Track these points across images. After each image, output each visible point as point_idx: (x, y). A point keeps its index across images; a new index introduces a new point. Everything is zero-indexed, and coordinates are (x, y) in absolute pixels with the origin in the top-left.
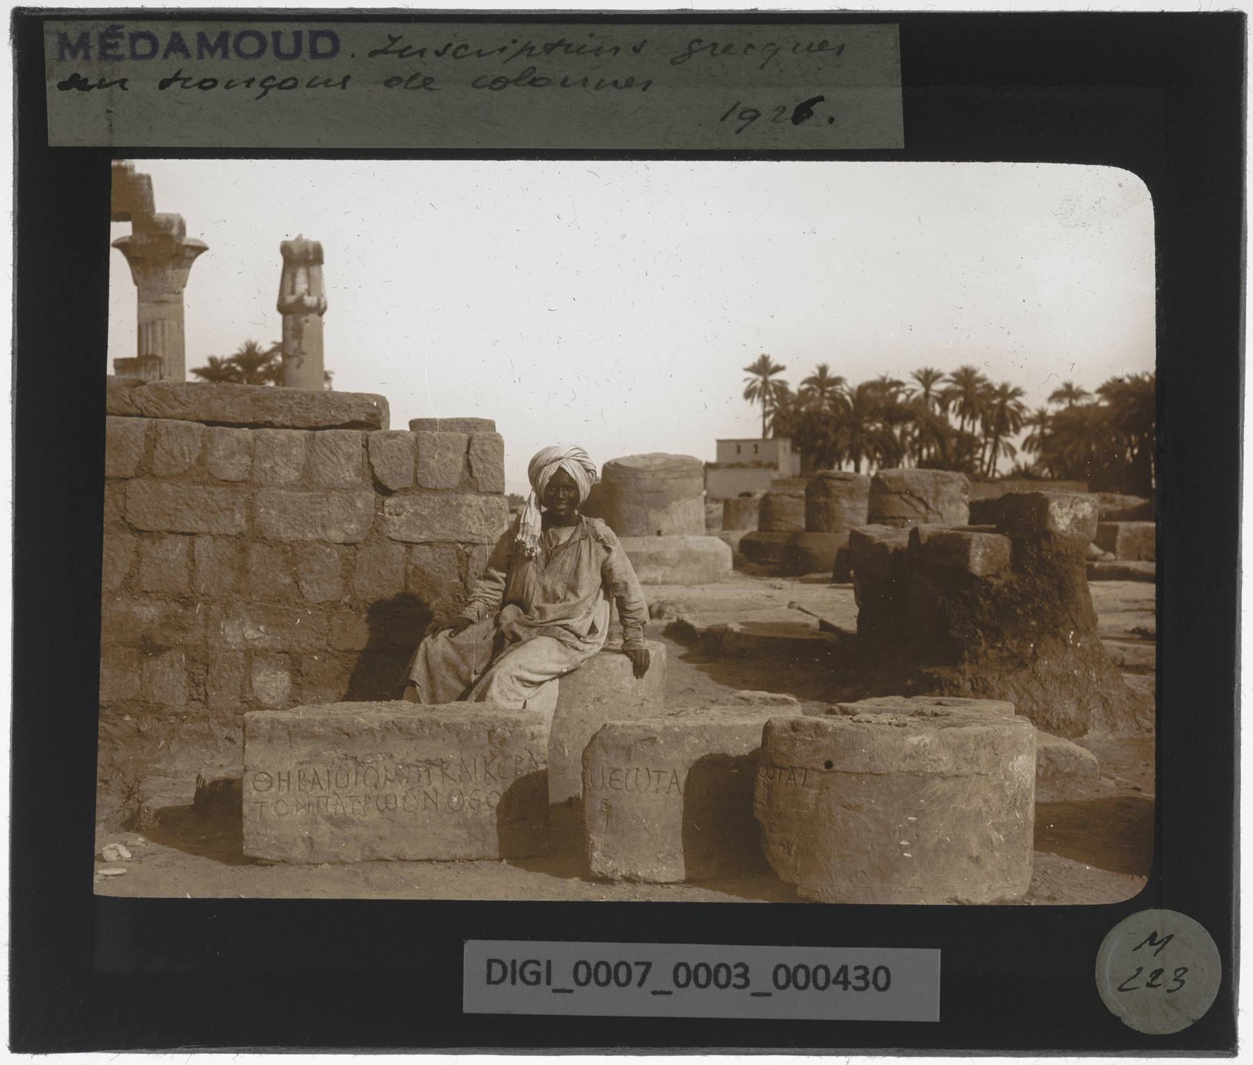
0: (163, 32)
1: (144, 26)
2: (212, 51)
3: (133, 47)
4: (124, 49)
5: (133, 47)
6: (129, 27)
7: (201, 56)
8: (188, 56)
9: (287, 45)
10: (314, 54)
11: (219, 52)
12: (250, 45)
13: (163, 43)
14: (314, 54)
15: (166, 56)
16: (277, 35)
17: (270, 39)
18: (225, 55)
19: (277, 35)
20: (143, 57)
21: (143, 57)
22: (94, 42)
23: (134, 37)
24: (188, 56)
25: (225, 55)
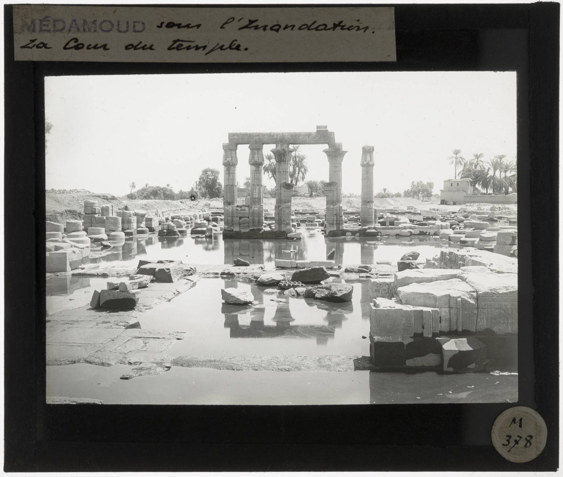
4: (51, 27)
5: (54, 26)
7: (84, 30)
12: (106, 26)
14: (134, 31)
17: (115, 24)
22: (37, 22)
23: (55, 21)
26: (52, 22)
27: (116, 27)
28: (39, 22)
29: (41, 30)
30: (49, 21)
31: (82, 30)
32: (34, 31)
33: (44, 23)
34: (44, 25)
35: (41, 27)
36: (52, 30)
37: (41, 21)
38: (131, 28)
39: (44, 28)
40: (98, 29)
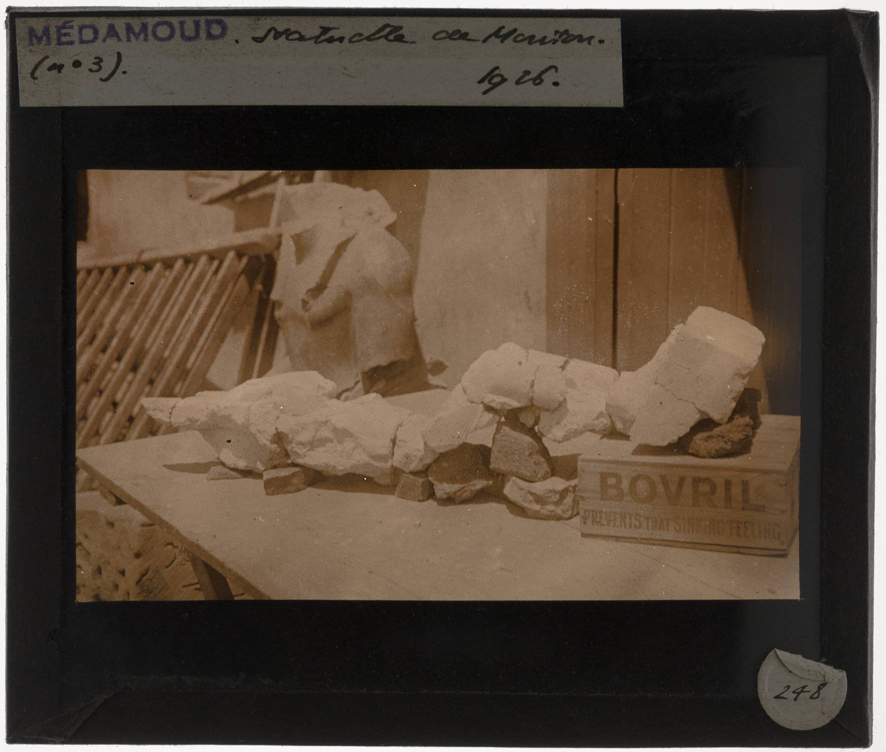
0: (103, 24)
1: (88, 21)
2: (137, 38)
3: (80, 32)
6: (77, 22)
7: (129, 40)
8: (119, 39)
9: (190, 30)
10: (210, 36)
11: (142, 36)
12: (163, 31)
13: (103, 32)
14: (210, 36)
15: (104, 40)
16: (182, 24)
17: (177, 26)
18: (146, 39)
19: (182, 24)
20: (87, 42)
21: (87, 42)
24: (119, 39)
25: (146, 39)
26: (76, 29)
27: (178, 33)
28: (55, 30)
29: (60, 43)
30: (72, 27)
31: (124, 39)
32: (49, 43)
33: (63, 31)
34: (65, 35)
35: (59, 39)
36: (77, 40)
37: (59, 29)
38: (203, 34)
39: (64, 39)
40: (151, 37)
